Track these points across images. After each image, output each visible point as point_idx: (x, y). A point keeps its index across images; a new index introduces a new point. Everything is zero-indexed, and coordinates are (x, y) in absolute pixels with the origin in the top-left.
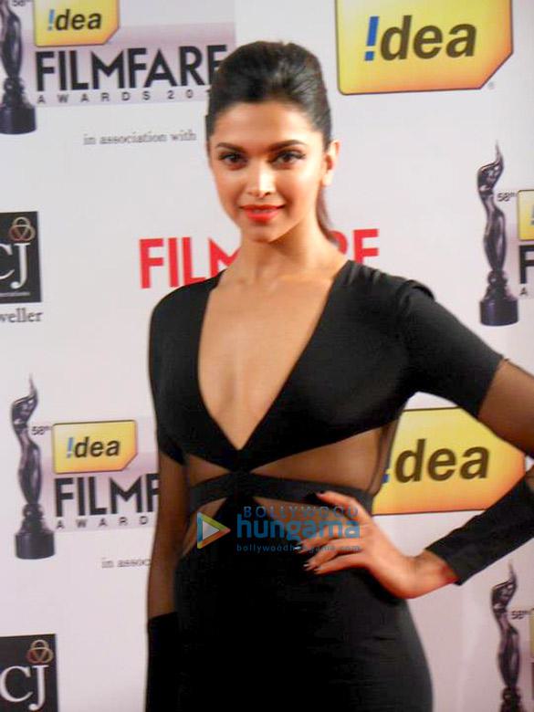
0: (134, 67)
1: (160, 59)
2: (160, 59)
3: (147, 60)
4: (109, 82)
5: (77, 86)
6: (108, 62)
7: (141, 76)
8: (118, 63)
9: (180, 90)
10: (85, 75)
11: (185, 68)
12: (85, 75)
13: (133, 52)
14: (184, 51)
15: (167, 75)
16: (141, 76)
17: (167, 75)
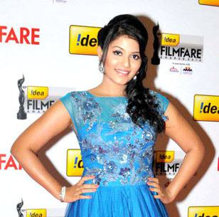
0: (182, 52)
1: (187, 51)
2: (187, 51)
3: (185, 51)
4: (176, 55)
5: (169, 55)
6: (176, 50)
7: (183, 54)
8: (178, 51)
9: (191, 59)
10: (171, 53)
11: (192, 54)
12: (171, 53)
13: (182, 49)
14: (192, 50)
15: (188, 55)
16: (183, 54)
17: (188, 55)
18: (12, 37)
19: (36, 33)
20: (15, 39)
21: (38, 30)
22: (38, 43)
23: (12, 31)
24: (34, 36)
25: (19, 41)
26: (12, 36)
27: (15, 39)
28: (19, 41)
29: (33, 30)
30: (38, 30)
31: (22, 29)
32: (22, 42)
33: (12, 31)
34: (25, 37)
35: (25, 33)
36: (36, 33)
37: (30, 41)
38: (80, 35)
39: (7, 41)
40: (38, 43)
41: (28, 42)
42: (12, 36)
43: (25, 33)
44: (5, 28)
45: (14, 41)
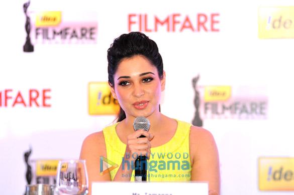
18: (187, 24)
19: (216, 18)
20: (191, 27)
21: (217, 15)
22: (217, 30)
23: (187, 19)
24: (213, 22)
27: (191, 27)
29: (213, 15)
30: (217, 15)
33: (187, 19)
36: (216, 18)
38: (270, 18)
39: (181, 30)
40: (217, 30)
43: (202, 19)
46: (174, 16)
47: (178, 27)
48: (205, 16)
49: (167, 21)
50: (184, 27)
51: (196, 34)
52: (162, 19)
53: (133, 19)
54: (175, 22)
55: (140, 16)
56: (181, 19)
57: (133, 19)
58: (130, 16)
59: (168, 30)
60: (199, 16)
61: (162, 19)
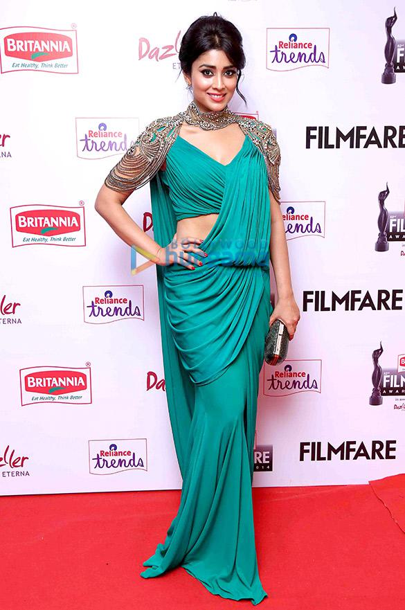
18: (373, 140)
20: (377, 142)
23: (374, 132)
25: (382, 145)
26: (373, 139)
27: (377, 142)
28: (382, 145)
31: (387, 128)
32: (386, 146)
33: (374, 132)
34: (391, 138)
35: (390, 133)
37: (397, 145)
39: (366, 146)
41: (394, 146)
42: (373, 139)
43: (390, 133)
44: (365, 128)
45: (376, 145)
46: (359, 128)
47: (363, 142)
48: (393, 128)
49: (351, 134)
50: (369, 142)
51: (383, 149)
52: (345, 135)
53: (313, 133)
54: (360, 137)
55: (321, 128)
56: (367, 133)
57: (313, 133)
58: (309, 129)
59: (352, 146)
60: (387, 128)
61: (345, 135)
